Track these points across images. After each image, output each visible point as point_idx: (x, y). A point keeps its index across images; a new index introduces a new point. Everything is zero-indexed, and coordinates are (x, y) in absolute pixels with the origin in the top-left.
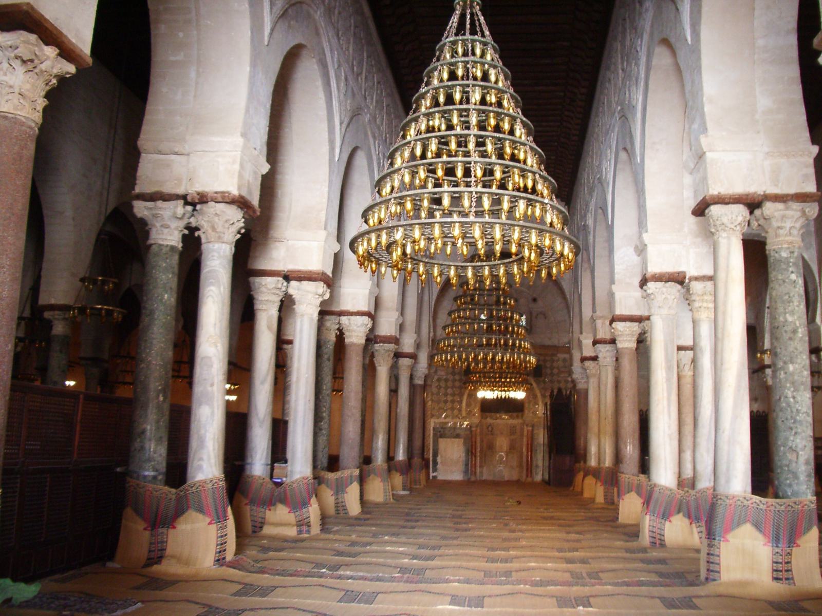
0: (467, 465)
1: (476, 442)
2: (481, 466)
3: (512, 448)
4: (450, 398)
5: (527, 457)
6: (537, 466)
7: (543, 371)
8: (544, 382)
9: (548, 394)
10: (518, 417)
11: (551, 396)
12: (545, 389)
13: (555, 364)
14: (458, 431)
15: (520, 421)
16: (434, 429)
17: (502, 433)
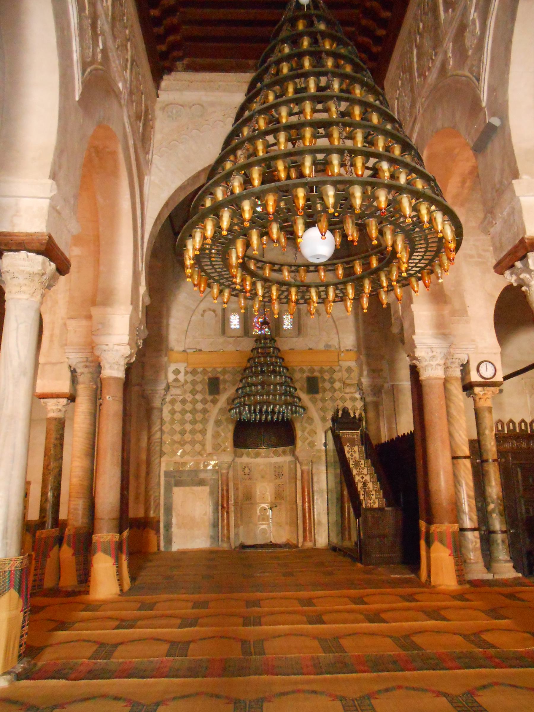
0: (215, 525)
1: (227, 491)
2: (237, 526)
3: (279, 496)
4: (188, 427)
5: (304, 509)
6: (320, 523)
7: (320, 385)
8: (323, 400)
9: (330, 415)
10: (284, 453)
11: (334, 419)
12: (323, 409)
13: (336, 376)
14: (202, 476)
15: (289, 458)
16: (167, 474)
17: (263, 477)
